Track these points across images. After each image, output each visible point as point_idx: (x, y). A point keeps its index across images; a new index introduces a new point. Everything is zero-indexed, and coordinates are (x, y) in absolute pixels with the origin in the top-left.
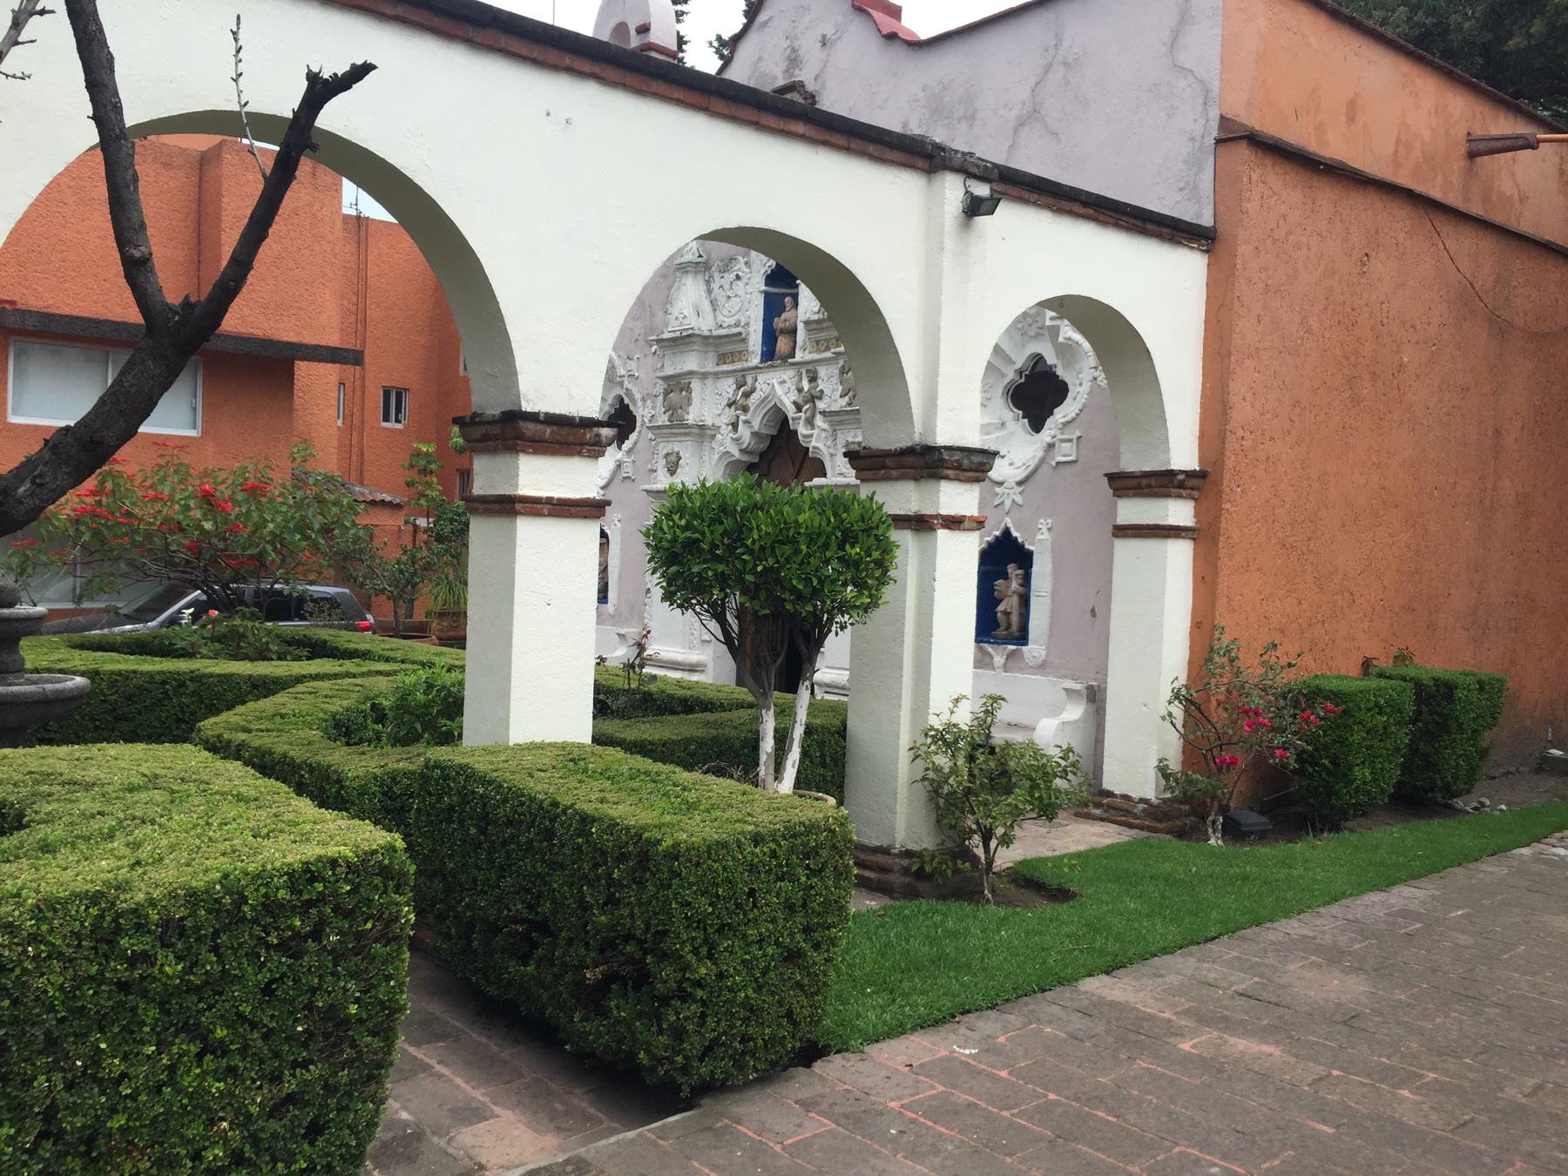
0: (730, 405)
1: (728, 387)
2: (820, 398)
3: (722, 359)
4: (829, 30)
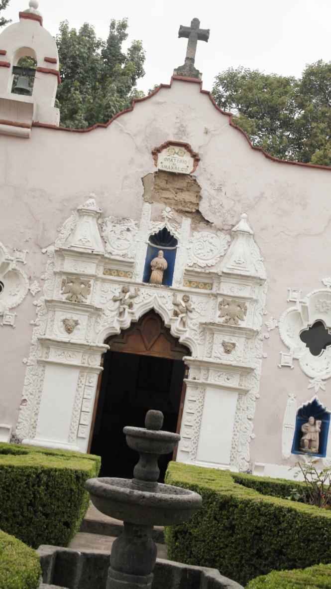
0: (115, 301)
1: (117, 290)
2: (191, 312)
3: (109, 272)
4: (210, 127)
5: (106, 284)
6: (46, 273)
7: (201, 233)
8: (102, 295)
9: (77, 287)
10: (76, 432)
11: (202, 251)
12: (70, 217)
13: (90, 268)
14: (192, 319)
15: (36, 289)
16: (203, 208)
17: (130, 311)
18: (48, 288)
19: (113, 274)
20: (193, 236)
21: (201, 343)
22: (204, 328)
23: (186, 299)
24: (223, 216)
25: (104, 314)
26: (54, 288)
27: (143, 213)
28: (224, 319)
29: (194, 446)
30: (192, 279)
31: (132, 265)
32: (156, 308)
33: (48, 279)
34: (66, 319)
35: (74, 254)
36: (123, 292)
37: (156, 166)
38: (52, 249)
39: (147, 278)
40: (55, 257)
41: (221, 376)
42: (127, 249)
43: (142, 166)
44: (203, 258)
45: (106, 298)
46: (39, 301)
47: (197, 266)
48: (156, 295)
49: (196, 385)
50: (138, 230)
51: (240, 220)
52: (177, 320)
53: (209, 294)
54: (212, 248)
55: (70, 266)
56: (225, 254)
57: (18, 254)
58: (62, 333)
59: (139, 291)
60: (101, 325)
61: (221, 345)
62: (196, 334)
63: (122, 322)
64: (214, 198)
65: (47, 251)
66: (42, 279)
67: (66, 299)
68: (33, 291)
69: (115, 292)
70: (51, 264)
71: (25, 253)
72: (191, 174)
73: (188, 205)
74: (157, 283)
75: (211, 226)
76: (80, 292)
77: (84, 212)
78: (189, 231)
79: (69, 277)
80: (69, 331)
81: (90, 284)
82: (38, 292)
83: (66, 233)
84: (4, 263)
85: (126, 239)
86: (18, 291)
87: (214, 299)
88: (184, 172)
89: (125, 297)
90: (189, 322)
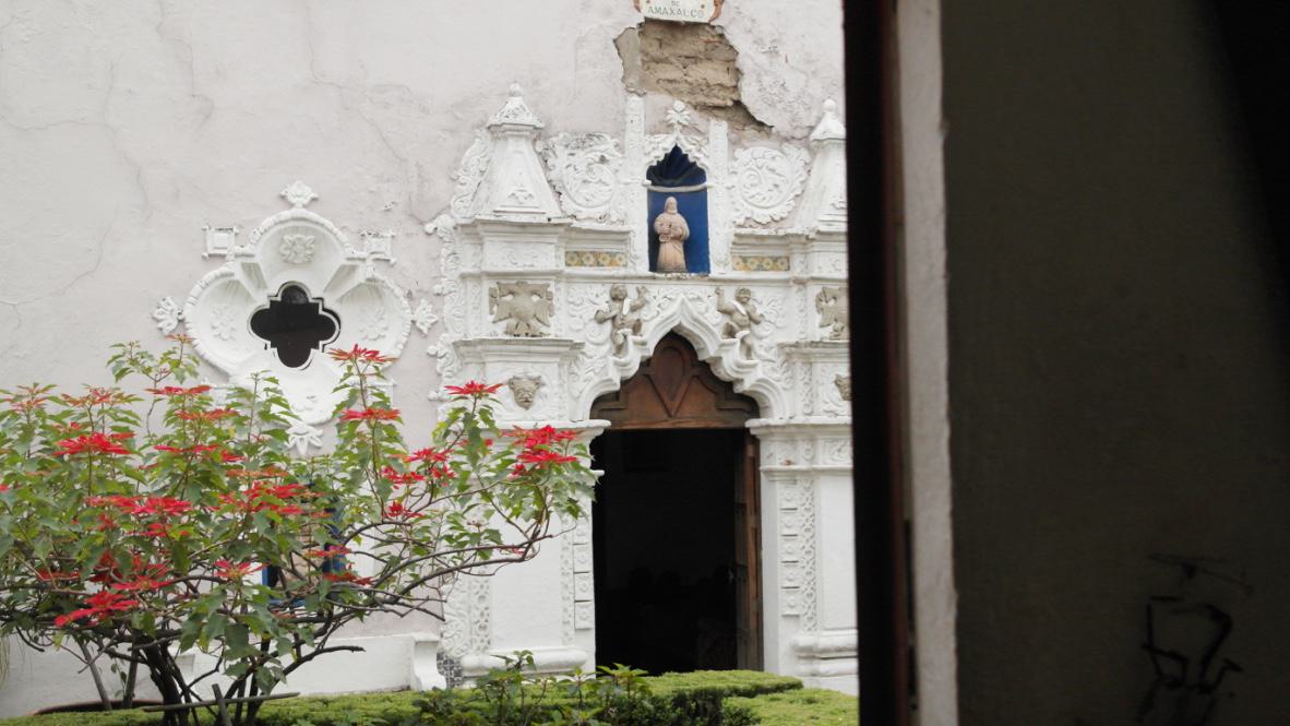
0: (601, 321)
2: (757, 323)
3: (575, 258)
5: (576, 286)
6: (443, 279)
7: (751, 149)
8: (574, 312)
9: (530, 303)
10: (571, 620)
11: (758, 190)
12: (474, 142)
13: (545, 257)
14: (761, 338)
15: (432, 318)
16: (749, 95)
17: (638, 338)
18: (454, 311)
19: (585, 262)
20: (736, 159)
21: (788, 386)
22: (788, 354)
23: (743, 297)
24: (789, 109)
25: (583, 353)
26: (466, 312)
27: (628, 119)
28: (830, 329)
29: (810, 601)
30: (749, 252)
31: (624, 237)
32: (685, 324)
33: (450, 292)
34: (515, 378)
35: (508, 229)
36: (615, 298)
37: (638, 9)
38: (445, 221)
39: (655, 264)
40: (457, 239)
41: (843, 449)
42: (607, 202)
43: (608, 13)
44: (762, 204)
45: (581, 317)
46: (439, 344)
47: (753, 223)
48: (682, 296)
49: (792, 477)
50: (623, 158)
51: (824, 114)
52: (734, 344)
53: (787, 281)
54: (778, 180)
55: (500, 256)
56: (803, 191)
57: (372, 243)
58: (511, 411)
59: (646, 291)
60: (581, 379)
61: (833, 385)
62: (773, 369)
63: (625, 365)
64: (767, 73)
65: (436, 229)
66: (438, 294)
67: (506, 333)
68: (422, 324)
69: (597, 301)
70: (451, 257)
71: (390, 239)
72: (713, 23)
73: (716, 92)
74: (677, 269)
75: (769, 134)
76: (532, 312)
77: (510, 130)
78: (726, 149)
79: (503, 282)
80: (525, 402)
81: (551, 293)
82: (433, 324)
83: (470, 181)
84: (343, 268)
85: (600, 181)
86: (386, 329)
87: (799, 290)
88: (697, 19)
89: (621, 310)
90: (756, 344)
